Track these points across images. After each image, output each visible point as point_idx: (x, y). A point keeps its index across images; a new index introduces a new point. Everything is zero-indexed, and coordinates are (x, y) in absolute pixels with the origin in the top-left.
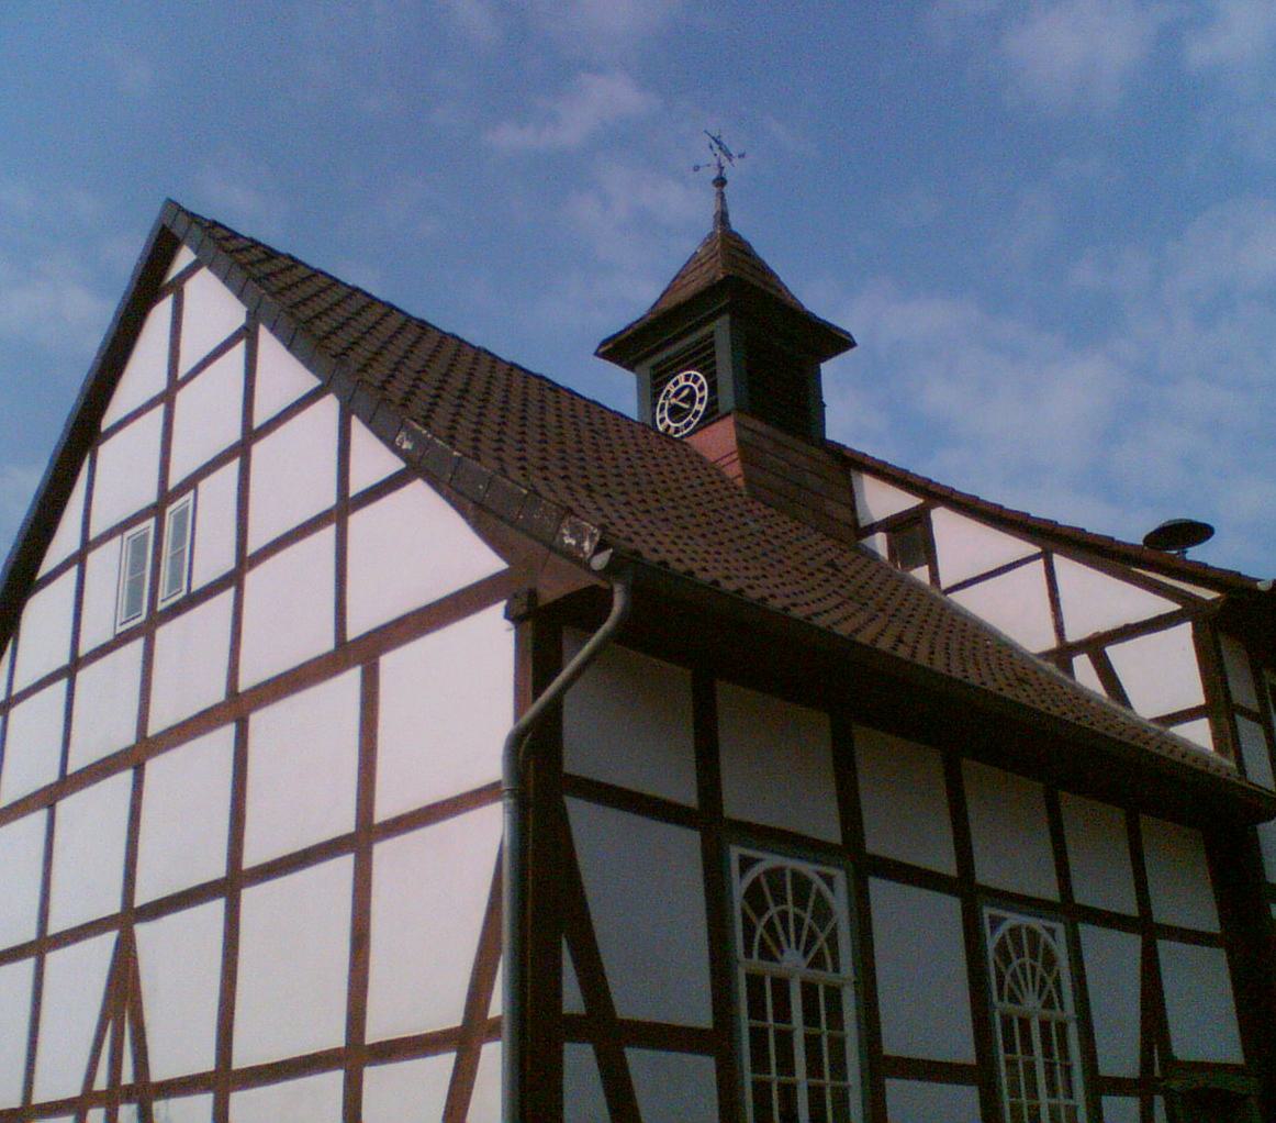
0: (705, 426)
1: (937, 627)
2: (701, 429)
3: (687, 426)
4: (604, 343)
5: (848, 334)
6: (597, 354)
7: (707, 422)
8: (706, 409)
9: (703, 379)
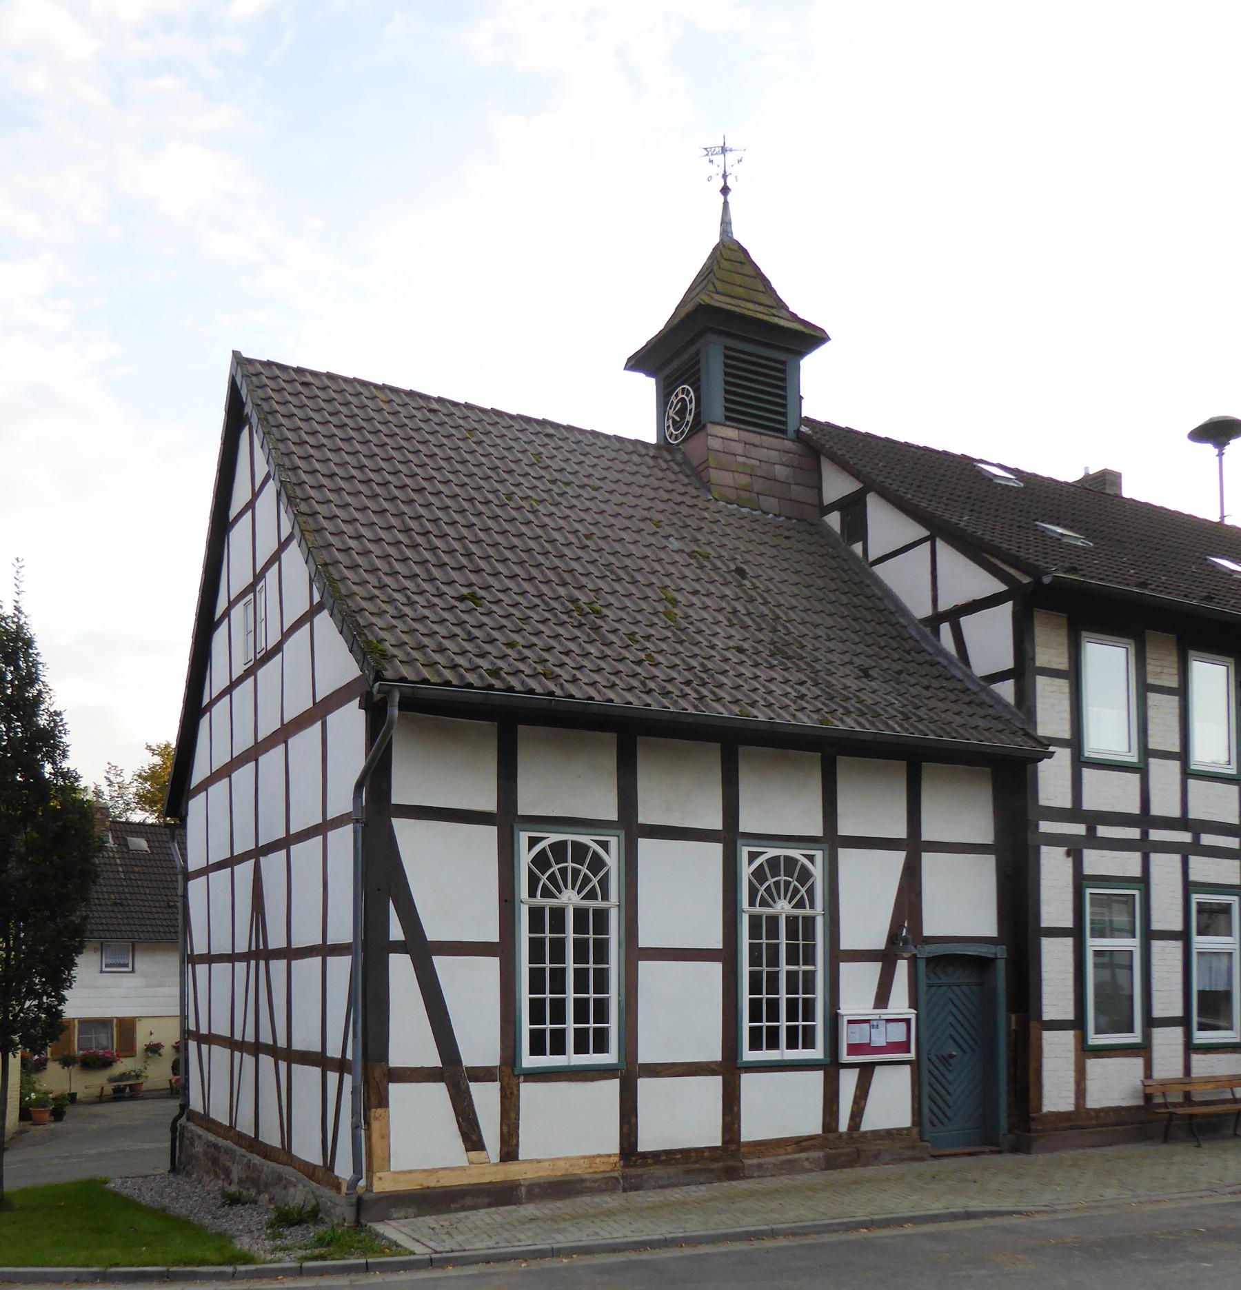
0: (694, 434)
1: (994, 529)
2: (691, 437)
3: (682, 433)
4: (629, 360)
5: (823, 331)
6: (625, 368)
7: (694, 431)
8: (693, 420)
9: (692, 393)
